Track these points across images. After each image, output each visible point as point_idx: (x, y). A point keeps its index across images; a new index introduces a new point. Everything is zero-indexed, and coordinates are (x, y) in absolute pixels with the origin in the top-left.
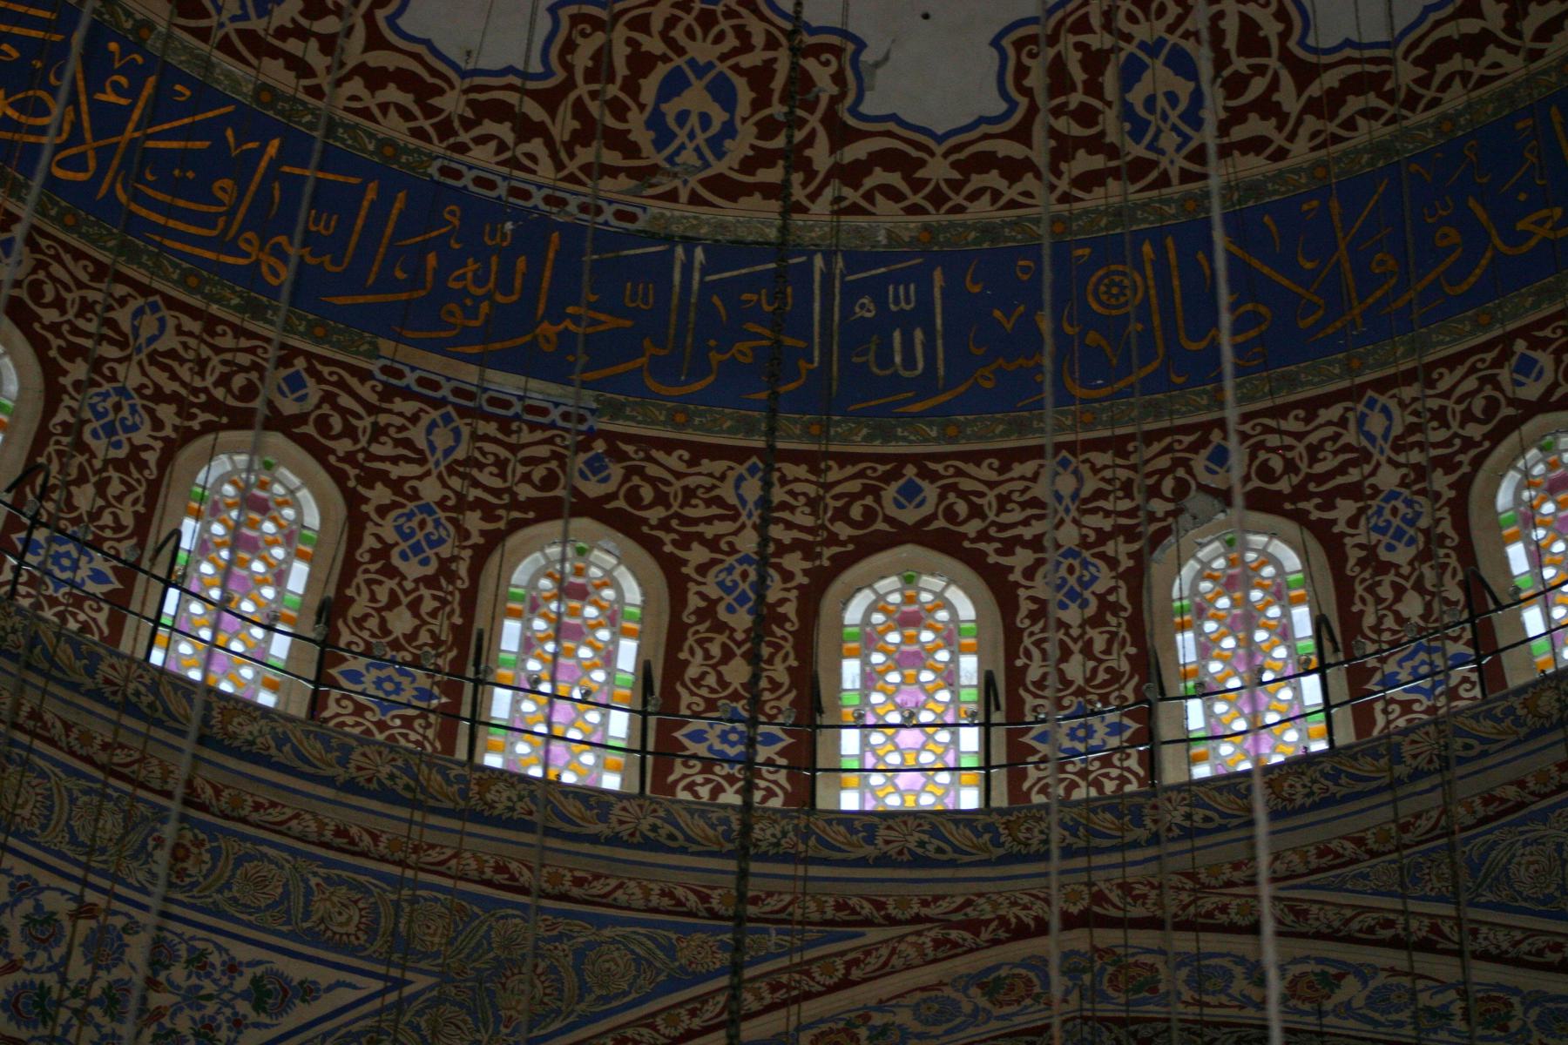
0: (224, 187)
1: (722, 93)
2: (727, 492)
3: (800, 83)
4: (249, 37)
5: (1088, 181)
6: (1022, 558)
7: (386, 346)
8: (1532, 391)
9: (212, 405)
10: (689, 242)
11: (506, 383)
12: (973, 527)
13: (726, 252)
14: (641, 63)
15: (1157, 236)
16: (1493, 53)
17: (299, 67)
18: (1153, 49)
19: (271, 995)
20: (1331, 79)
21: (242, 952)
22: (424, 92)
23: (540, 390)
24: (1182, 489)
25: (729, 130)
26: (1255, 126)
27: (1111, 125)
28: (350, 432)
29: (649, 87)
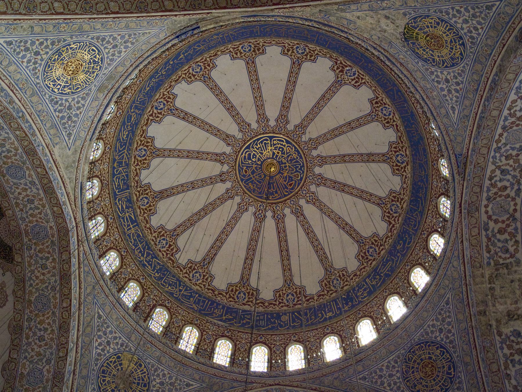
0: (192, 299)
1: (245, 294)
2: (242, 336)
3: (253, 294)
4: (196, 284)
5: (282, 306)
6: (273, 346)
7: (207, 317)
8: (328, 332)
9: (188, 322)
10: (240, 310)
11: (220, 323)
12: (268, 342)
13: (244, 311)
14: (236, 290)
15: (289, 313)
16: (325, 296)
17: (200, 287)
18: (290, 293)
19: (188, 385)
20: (308, 298)
21: (186, 380)
22: (214, 291)
23: (223, 324)
24: (290, 340)
25: (245, 298)
28: (202, 326)
29: (237, 293)
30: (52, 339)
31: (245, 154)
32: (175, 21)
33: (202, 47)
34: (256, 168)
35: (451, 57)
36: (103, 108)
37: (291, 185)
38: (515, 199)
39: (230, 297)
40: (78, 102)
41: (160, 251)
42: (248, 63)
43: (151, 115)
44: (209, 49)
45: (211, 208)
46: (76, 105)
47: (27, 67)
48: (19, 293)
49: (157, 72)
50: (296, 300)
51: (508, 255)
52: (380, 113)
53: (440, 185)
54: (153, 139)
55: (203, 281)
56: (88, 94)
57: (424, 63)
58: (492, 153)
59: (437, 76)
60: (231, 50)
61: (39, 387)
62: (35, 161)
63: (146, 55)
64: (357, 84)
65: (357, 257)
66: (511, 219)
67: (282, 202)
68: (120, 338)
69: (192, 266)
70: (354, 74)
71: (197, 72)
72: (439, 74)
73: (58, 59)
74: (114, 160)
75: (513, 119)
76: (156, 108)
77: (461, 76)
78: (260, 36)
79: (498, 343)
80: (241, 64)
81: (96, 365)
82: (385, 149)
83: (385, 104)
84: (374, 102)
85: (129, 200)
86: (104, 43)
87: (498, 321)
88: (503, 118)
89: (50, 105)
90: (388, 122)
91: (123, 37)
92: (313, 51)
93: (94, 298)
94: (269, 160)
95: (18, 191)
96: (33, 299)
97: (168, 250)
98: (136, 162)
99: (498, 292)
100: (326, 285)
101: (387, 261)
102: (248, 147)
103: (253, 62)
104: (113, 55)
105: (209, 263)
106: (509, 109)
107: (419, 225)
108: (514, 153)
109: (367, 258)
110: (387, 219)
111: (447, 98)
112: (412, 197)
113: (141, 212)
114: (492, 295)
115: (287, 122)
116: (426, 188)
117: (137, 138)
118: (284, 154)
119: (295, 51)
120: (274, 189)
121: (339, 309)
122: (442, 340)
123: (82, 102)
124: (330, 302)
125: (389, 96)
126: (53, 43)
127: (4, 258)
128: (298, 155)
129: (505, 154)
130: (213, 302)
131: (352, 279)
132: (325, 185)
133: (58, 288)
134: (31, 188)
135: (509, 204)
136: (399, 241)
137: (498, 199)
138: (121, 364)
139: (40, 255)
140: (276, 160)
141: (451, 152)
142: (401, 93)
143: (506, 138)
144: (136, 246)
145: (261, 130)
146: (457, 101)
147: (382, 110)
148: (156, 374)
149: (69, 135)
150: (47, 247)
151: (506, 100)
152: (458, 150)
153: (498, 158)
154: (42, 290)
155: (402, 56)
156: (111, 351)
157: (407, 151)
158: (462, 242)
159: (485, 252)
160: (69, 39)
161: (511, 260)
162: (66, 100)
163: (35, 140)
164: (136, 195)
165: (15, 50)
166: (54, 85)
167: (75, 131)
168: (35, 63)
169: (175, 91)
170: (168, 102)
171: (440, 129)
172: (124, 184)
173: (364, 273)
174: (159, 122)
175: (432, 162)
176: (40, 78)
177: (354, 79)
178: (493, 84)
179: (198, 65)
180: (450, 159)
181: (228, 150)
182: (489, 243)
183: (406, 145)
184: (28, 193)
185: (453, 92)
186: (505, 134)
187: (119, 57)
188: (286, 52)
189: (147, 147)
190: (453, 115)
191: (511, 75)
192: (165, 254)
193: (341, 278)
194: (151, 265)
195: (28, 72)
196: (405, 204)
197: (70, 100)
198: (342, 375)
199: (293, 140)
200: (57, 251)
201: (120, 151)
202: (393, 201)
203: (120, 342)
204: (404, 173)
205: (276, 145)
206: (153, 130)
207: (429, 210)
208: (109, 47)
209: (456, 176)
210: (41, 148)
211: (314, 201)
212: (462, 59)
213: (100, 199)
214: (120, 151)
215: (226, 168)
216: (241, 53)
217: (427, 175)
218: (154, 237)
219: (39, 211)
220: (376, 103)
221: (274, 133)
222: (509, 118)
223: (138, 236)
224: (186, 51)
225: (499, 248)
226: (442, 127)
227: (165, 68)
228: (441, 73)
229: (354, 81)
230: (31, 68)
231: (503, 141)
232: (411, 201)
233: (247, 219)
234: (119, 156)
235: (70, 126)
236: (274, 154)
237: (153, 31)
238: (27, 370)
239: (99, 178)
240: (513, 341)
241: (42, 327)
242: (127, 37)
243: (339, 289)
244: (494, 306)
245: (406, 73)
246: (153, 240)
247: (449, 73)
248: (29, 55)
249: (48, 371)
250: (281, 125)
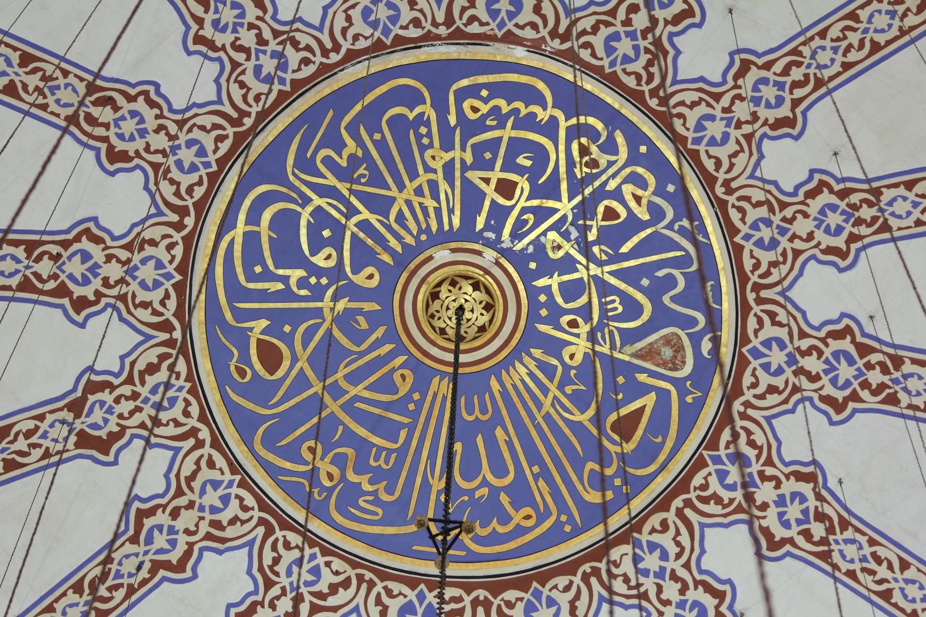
31: (254, 218)
34: (344, 320)
37: (625, 427)
94: (442, 255)
102: (269, 167)
118: (551, 190)
120: (500, 472)
128: (660, 191)
132: (893, 400)
140: (493, 245)
145: (360, 26)
181: (122, 202)
199: (612, 81)
205: (480, 126)
211: (818, 530)
221: (458, 36)
236: (472, 198)
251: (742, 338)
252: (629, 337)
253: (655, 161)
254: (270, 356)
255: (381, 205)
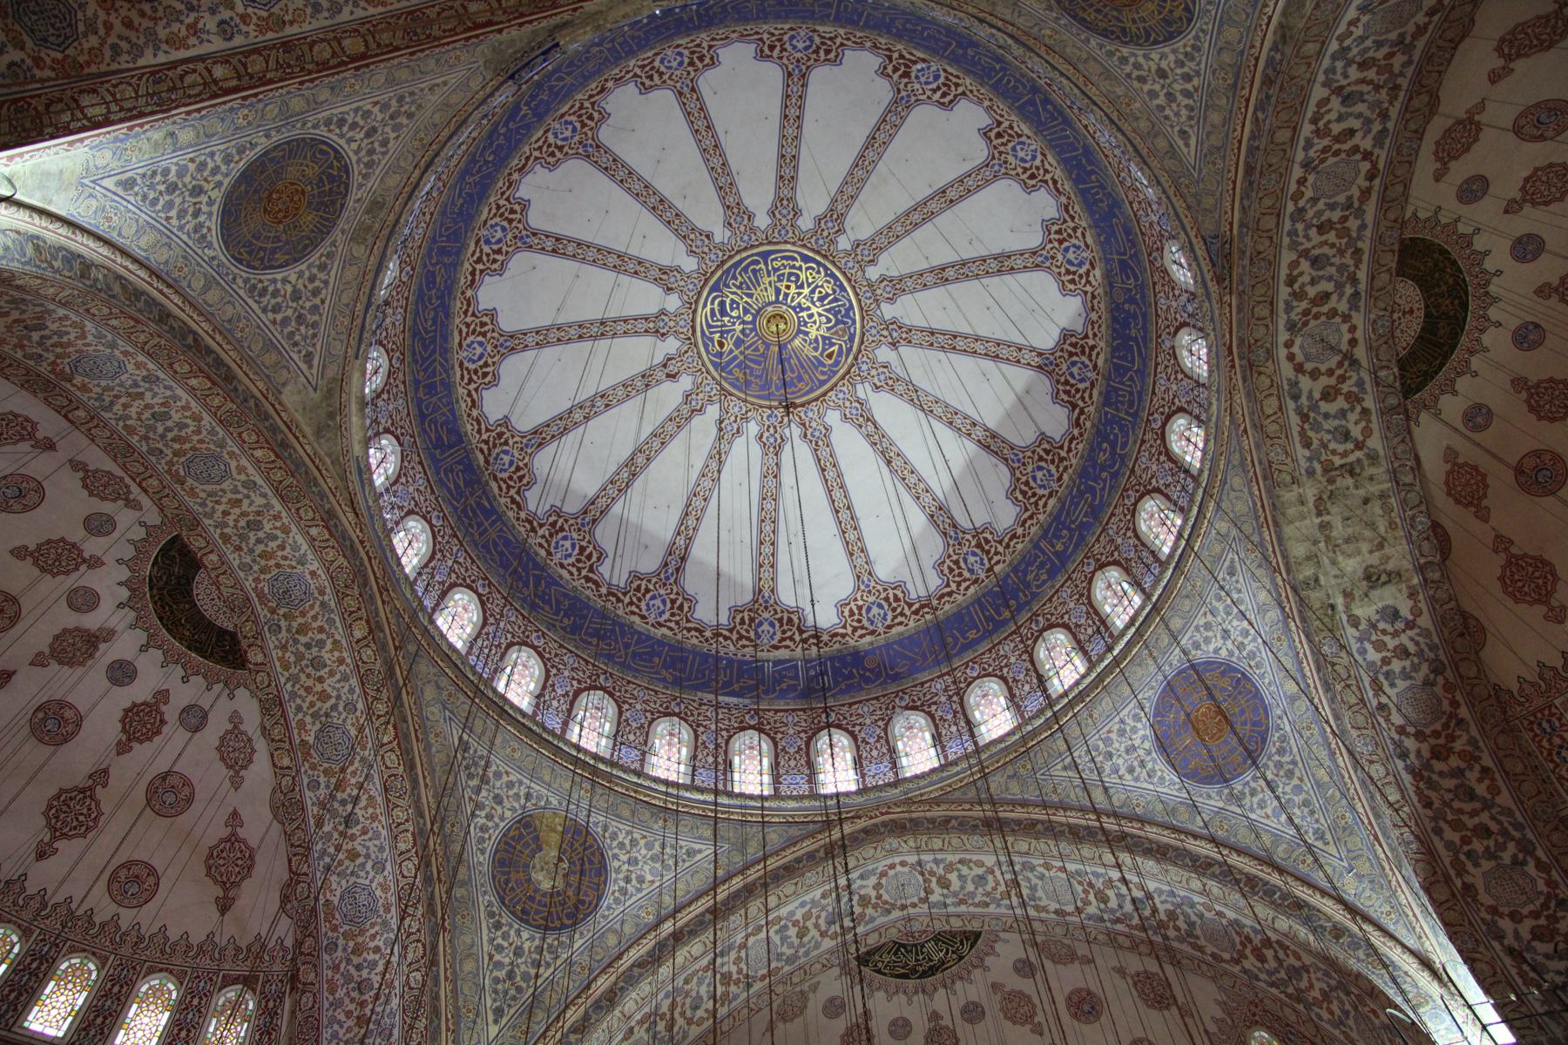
0: (656, 660)
3: (790, 621)
5: (862, 636)
13: (777, 663)
17: (671, 629)
26: (900, 619)
27: (865, 623)
30: (374, 818)
32: (501, 43)
33: (569, 80)
34: (743, 331)
35: (1164, 20)
36: (369, 277)
37: (830, 356)
38: (1350, 316)
39: (741, 637)
40: (312, 279)
41: (562, 566)
42: (681, 94)
43: (479, 260)
44: (586, 78)
45: (656, 444)
46: (310, 287)
47: (181, 228)
48: (277, 732)
49: (473, 160)
50: (889, 617)
51: (1350, 446)
52: (1011, 159)
53: (1174, 304)
54: (492, 314)
55: (673, 615)
56: (330, 256)
57: (1101, 40)
58: (1288, 225)
59: (1137, 66)
60: (638, 71)
61: (373, 925)
62: (244, 435)
63: (446, 133)
64: (946, 100)
65: (1010, 495)
66: (1346, 364)
67: (816, 399)
68: (521, 783)
69: (639, 585)
70: (937, 77)
71: (565, 139)
72: (1141, 60)
73: (247, 192)
74: (417, 382)
75: (1326, 142)
76: (488, 242)
77: (1192, 59)
78: (698, 28)
79: (1352, 641)
80: (664, 99)
81: (483, 853)
82: (1034, 239)
83: (1019, 136)
84: (992, 135)
85: (468, 466)
86: (345, 129)
87: (1348, 595)
88: (1302, 143)
89: (250, 301)
90: (1032, 177)
91: (385, 107)
92: (831, 39)
93: (445, 708)
94: (770, 309)
95: (221, 508)
96: (311, 739)
97: (579, 561)
98: (466, 377)
99: (1339, 531)
100: (951, 570)
101: (1081, 494)
102: (715, 288)
103: (693, 90)
104: (371, 152)
105: (677, 570)
106: (1314, 121)
107: (1140, 401)
108: (1336, 215)
109: (1034, 495)
110: (1066, 398)
111: (1167, 112)
112: (1114, 339)
113: (500, 489)
114: (1328, 539)
115: (797, 213)
116: (1144, 315)
117: (457, 321)
118: (801, 287)
119: (787, 46)
121: (989, 619)
122: (1231, 654)
123: (323, 276)
124: (967, 608)
125: (1026, 118)
126: (228, 159)
127: (223, 660)
129: (1315, 221)
130: (705, 657)
131: (1008, 546)
133: (360, 706)
134: (248, 497)
135: (1338, 330)
136: (1100, 444)
137: (1313, 323)
138: (537, 838)
139: (303, 639)
141: (1192, 234)
142: (1055, 108)
143: (1314, 186)
144: (505, 567)
146: (1190, 118)
147: (1014, 149)
148: (615, 844)
149: (308, 359)
150: (315, 618)
151: (1304, 103)
152: (1208, 226)
153: (1301, 234)
154: (327, 715)
155: (1048, 32)
156: (508, 814)
157: (1088, 235)
158: (1245, 431)
159: (1298, 446)
160: (263, 140)
161: (1359, 454)
162: (285, 281)
163: (236, 389)
164: (482, 450)
165: (145, 197)
166: (250, 253)
167: (318, 347)
168: (196, 214)
169: (523, 192)
170: (510, 221)
171: (1159, 183)
172: (449, 431)
173: (1033, 530)
174: (500, 271)
175: (1150, 255)
176: (216, 245)
177: (939, 88)
178: (1270, 72)
179: (567, 123)
180: (1192, 250)
181: (673, 303)
182: (1306, 426)
183: (1084, 224)
184: (245, 508)
185: (1180, 97)
186: (1311, 178)
187: (384, 154)
188: (767, 51)
189: (484, 334)
190: (1185, 150)
191: (1310, 45)
192: (574, 570)
193: (983, 550)
194: (549, 603)
195: (184, 237)
196: (1102, 357)
197: (293, 278)
198: (1024, 767)
200: (338, 624)
201: (424, 360)
202: (1071, 354)
203: (523, 791)
204: (1088, 288)
206: (490, 294)
207: (1157, 364)
208: (358, 137)
209: (1213, 287)
210: (252, 403)
212: (1190, 21)
213: (403, 480)
214: (424, 360)
215: (672, 345)
216: (661, 74)
217: (1143, 286)
218: (543, 536)
219: (279, 542)
220: (999, 135)
222: (1316, 141)
223: (507, 543)
224: (533, 97)
225: (1329, 432)
226: (1162, 180)
227: (491, 144)
228: (1146, 57)
229: (939, 93)
230: (190, 227)
231: (1309, 193)
232: (1114, 350)
233: (745, 454)
234: (425, 370)
235: (305, 338)
237: (453, 79)
238: (338, 893)
239: (392, 433)
240: (1384, 632)
241: (345, 796)
242: (394, 103)
243: (983, 576)
244: (1334, 563)
245: (1064, 67)
246: (541, 545)
247: (1163, 56)
248: (178, 201)
249: (385, 888)
250: (784, 222)
251: (863, 327)
252: (829, 329)
253: (833, 276)
254: (721, 345)
255: (750, 296)
